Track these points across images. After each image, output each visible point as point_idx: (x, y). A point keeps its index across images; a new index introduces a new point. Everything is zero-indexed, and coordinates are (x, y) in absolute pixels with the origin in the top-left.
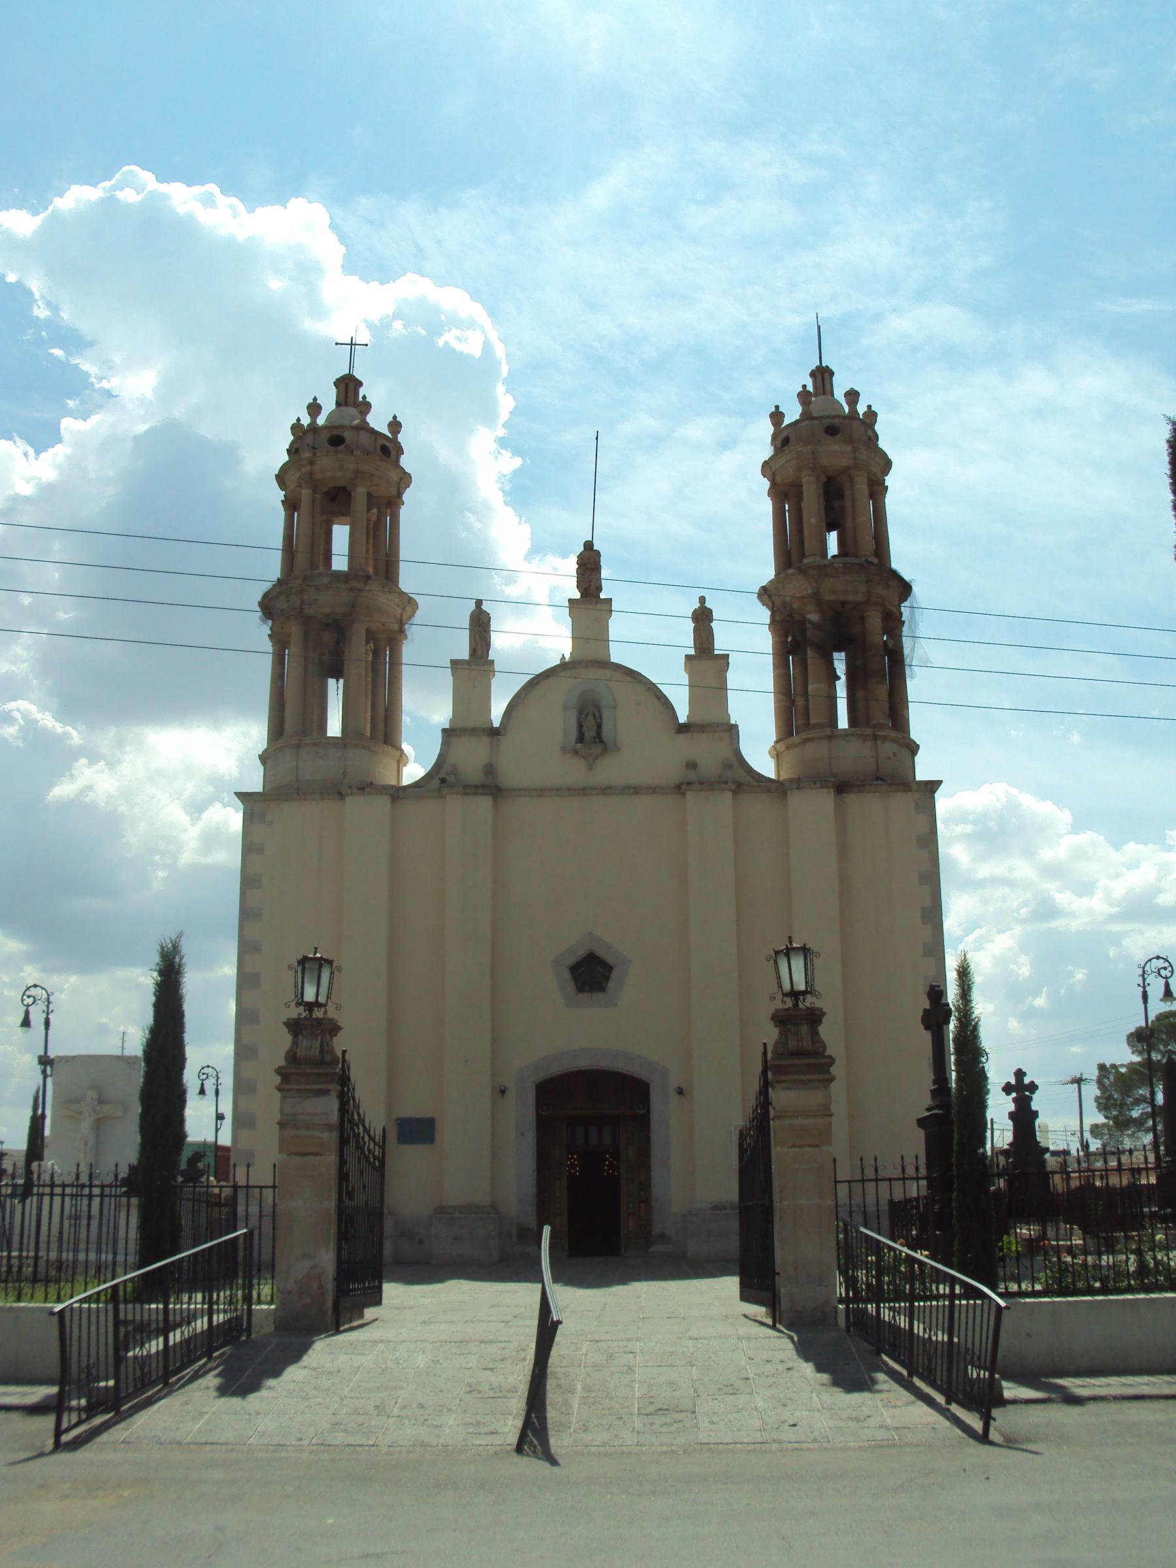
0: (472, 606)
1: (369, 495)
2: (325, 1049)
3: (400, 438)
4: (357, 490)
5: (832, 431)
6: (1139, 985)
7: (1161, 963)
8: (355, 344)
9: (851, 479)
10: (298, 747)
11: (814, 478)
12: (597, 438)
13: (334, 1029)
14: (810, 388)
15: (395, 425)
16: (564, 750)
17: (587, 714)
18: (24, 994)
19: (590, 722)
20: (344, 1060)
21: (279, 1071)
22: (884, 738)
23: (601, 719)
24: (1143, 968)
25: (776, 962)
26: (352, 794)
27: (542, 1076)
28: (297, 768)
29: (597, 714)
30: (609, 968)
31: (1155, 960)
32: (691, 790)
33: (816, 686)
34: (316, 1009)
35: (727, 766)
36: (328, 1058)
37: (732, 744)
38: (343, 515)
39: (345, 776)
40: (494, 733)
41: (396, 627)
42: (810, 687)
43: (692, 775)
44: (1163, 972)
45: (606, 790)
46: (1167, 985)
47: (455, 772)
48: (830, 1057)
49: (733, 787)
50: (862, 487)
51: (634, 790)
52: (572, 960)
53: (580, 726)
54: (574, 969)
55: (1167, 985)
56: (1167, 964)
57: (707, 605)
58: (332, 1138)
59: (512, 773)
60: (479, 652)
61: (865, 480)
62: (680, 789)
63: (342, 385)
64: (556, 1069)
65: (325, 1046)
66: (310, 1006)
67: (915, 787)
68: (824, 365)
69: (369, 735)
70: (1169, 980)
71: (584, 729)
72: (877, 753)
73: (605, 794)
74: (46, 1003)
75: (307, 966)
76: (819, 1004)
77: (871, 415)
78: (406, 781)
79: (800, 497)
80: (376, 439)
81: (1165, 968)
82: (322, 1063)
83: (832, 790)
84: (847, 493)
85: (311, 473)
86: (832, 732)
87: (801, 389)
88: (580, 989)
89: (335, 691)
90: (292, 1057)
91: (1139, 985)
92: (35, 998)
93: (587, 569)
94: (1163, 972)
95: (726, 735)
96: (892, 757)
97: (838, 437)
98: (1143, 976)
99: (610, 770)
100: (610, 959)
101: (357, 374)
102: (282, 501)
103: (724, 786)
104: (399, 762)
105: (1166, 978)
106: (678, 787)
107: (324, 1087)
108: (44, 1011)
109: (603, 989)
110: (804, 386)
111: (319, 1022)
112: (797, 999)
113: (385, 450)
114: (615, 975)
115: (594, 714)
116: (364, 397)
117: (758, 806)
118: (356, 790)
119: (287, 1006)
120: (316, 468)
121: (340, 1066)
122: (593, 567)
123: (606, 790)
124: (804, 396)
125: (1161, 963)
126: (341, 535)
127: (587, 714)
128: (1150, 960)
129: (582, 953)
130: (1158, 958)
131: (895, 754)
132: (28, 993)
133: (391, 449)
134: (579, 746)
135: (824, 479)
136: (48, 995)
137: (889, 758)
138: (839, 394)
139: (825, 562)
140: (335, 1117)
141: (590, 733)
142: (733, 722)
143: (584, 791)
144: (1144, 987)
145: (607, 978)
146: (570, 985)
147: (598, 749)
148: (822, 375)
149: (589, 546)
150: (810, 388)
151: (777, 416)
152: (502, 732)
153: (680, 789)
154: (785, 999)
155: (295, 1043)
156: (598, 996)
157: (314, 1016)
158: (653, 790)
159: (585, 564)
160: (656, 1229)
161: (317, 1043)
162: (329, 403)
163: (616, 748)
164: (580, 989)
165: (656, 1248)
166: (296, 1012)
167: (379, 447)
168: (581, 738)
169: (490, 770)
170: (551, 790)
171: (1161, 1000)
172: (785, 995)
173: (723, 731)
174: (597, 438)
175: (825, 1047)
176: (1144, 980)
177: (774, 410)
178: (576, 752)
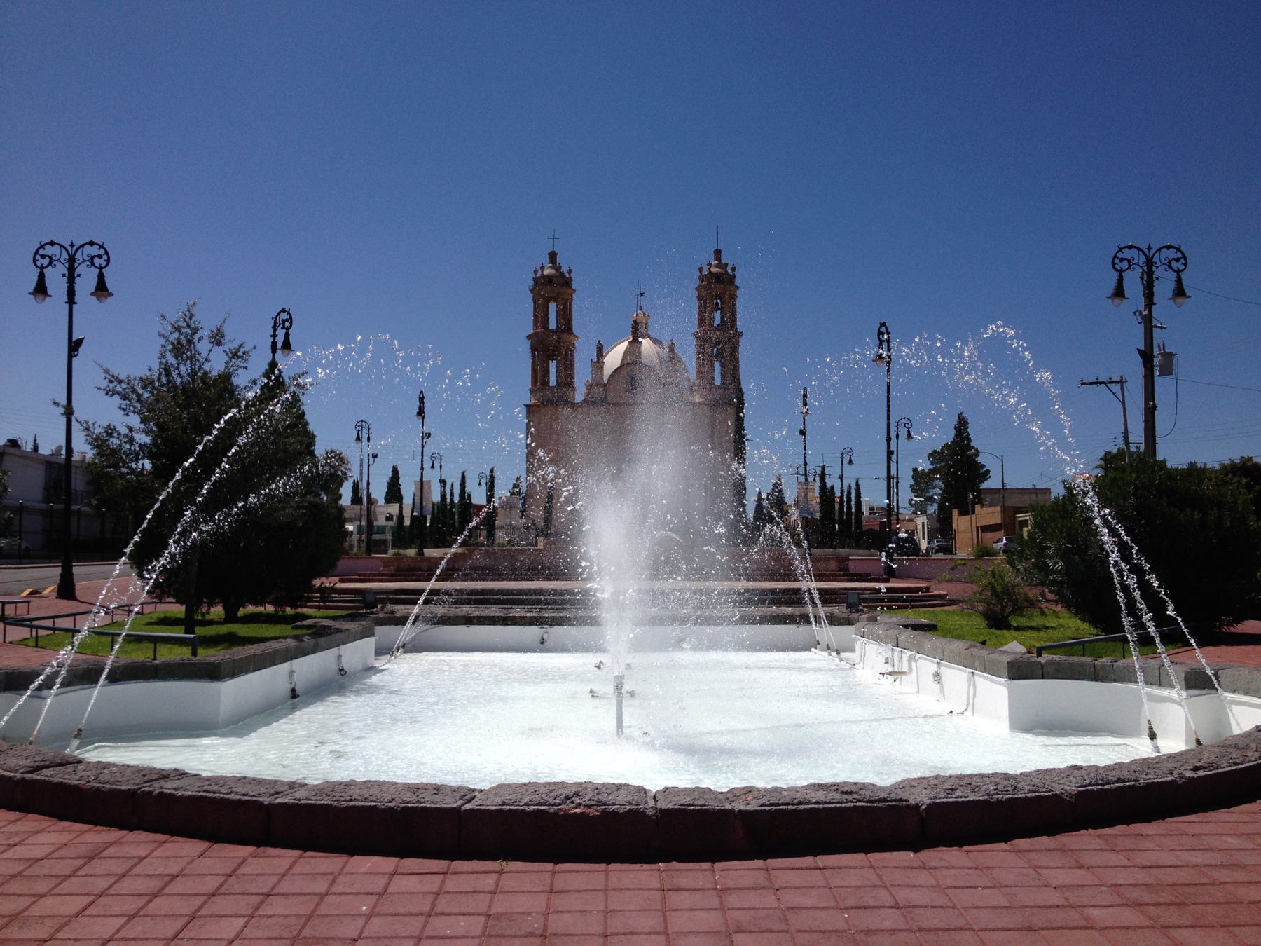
15: (570, 271)
40: (604, 385)
77: (733, 269)
89: (553, 365)
126: (553, 307)
151: (701, 269)
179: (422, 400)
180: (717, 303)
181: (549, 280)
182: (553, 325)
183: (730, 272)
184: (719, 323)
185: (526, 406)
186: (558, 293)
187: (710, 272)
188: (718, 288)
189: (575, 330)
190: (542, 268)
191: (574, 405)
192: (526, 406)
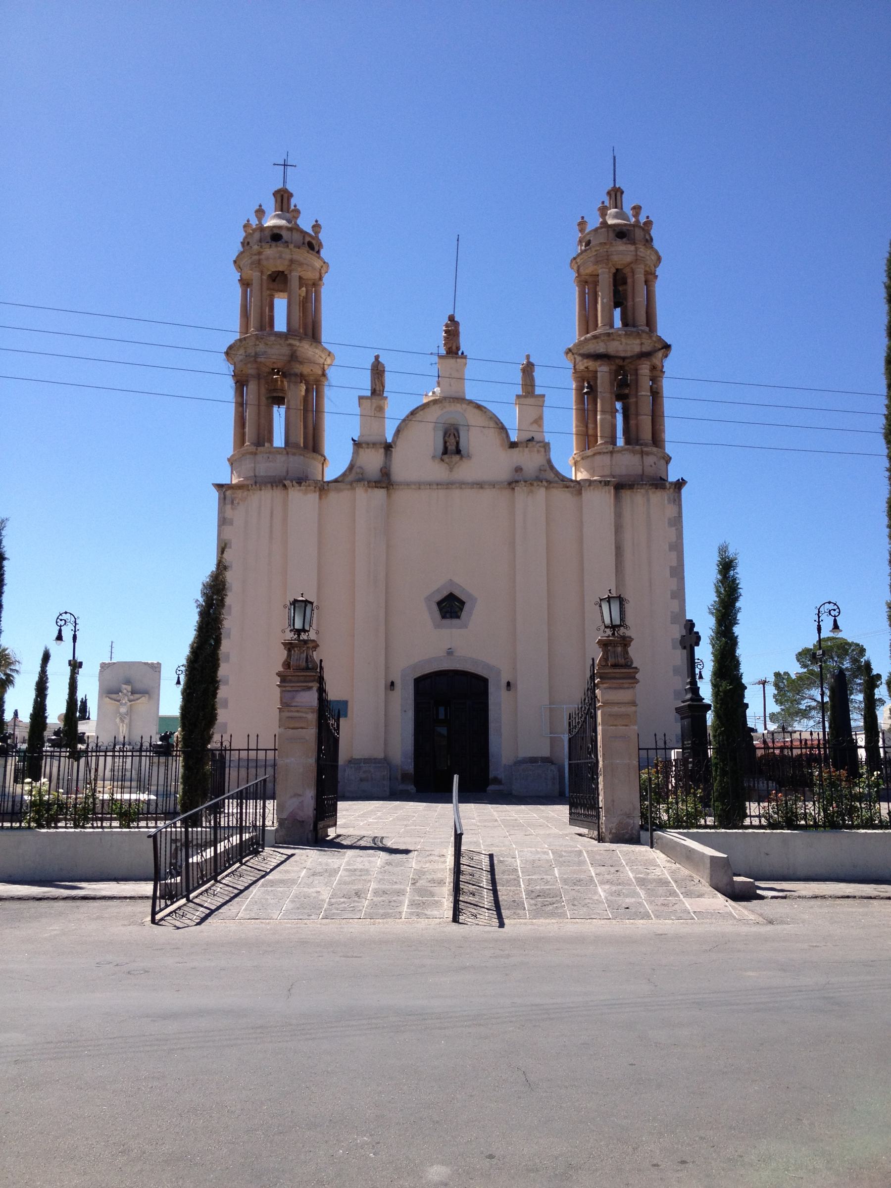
0: (373, 360)
1: (300, 278)
3: (321, 236)
4: (292, 274)
7: (831, 606)
8: (287, 165)
9: (633, 272)
10: (255, 454)
11: (607, 270)
15: (317, 227)
16: (434, 457)
17: (450, 434)
18: (58, 618)
19: (452, 441)
20: (321, 668)
21: (279, 674)
22: (648, 454)
23: (459, 438)
24: (819, 609)
25: (601, 606)
28: (255, 467)
29: (456, 435)
30: (463, 603)
32: (518, 486)
34: (302, 633)
35: (541, 470)
36: (310, 666)
38: (281, 291)
40: (388, 448)
41: (320, 372)
44: (833, 613)
45: (462, 485)
46: (835, 621)
48: (636, 668)
50: (640, 277)
51: (480, 485)
52: (439, 597)
53: (445, 443)
54: (439, 604)
55: (835, 621)
56: (835, 607)
57: (531, 360)
58: (312, 717)
62: (512, 484)
65: (309, 657)
66: (298, 632)
68: (617, 186)
69: (302, 445)
71: (448, 444)
72: (643, 462)
73: (461, 488)
74: (74, 624)
75: (296, 605)
76: (628, 633)
77: (649, 223)
78: (327, 478)
79: (596, 283)
80: (304, 237)
81: (834, 610)
82: (307, 669)
83: (612, 488)
84: (629, 281)
86: (613, 448)
88: (444, 617)
89: (279, 415)
90: (287, 664)
92: (65, 621)
94: (833, 613)
96: (653, 465)
97: (624, 240)
98: (818, 615)
100: (463, 598)
101: (290, 188)
104: (323, 464)
106: (510, 484)
108: (72, 630)
109: (458, 617)
110: (603, 203)
111: (305, 642)
112: (614, 630)
113: (311, 246)
114: (466, 608)
115: (454, 434)
116: (295, 206)
117: (561, 496)
120: (263, 257)
121: (318, 670)
123: (462, 485)
125: (831, 606)
126: (281, 305)
127: (450, 434)
128: (824, 604)
129: (445, 593)
130: (830, 603)
131: (655, 463)
132: (60, 617)
133: (315, 244)
135: (613, 270)
136: (75, 619)
137: (651, 466)
138: (627, 209)
140: (315, 703)
141: (452, 447)
142: (547, 441)
143: (448, 485)
144: (819, 622)
145: (461, 610)
147: (456, 458)
149: (452, 318)
150: (607, 204)
151: (582, 224)
152: (393, 446)
153: (512, 484)
154: (606, 629)
155: (289, 655)
157: (301, 638)
158: (493, 485)
160: (491, 776)
163: (469, 457)
164: (444, 617)
165: (491, 788)
166: (290, 636)
168: (445, 452)
171: (830, 631)
172: (606, 627)
175: (632, 663)
176: (819, 617)
178: (442, 460)
181: (275, 236)
182: (280, 325)
185: (219, 487)
186: (292, 261)
187: (604, 224)
188: (623, 252)
189: (327, 334)
190: (260, 212)
191: (323, 488)
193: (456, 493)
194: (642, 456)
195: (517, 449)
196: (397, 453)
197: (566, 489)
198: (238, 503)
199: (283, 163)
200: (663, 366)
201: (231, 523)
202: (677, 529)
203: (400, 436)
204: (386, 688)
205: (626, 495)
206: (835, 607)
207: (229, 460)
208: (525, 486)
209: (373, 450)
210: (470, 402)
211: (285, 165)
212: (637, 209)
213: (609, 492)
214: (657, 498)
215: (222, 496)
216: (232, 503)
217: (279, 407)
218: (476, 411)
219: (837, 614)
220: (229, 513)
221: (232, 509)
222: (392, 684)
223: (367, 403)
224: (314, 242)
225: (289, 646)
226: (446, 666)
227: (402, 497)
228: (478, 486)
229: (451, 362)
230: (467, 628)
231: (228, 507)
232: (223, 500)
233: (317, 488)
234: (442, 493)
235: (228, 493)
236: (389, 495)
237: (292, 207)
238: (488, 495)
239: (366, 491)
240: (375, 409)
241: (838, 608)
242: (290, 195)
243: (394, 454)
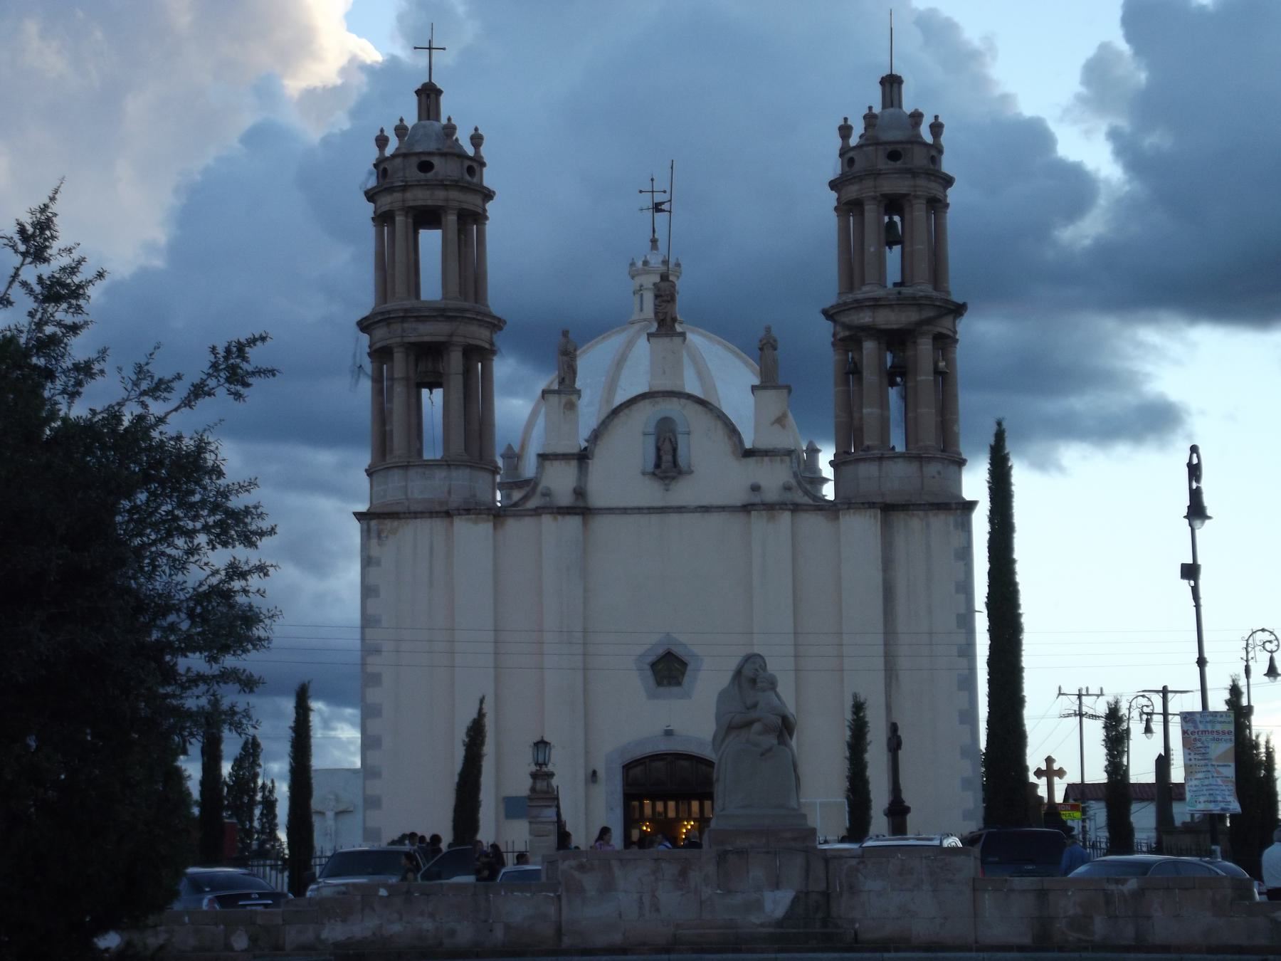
2: (549, 785)
3: (484, 151)
4: (449, 218)
5: (894, 156)
6: (1242, 658)
7: (1266, 636)
12: (672, 168)
13: (551, 775)
14: (877, 109)
15: (477, 140)
17: (665, 439)
19: (667, 447)
23: (677, 444)
24: (1247, 640)
26: (459, 514)
27: (628, 757)
29: (673, 440)
30: (684, 665)
31: (1261, 632)
32: (755, 510)
33: (869, 410)
34: (544, 766)
35: (787, 488)
37: (792, 467)
39: (449, 493)
40: (583, 457)
42: (864, 411)
43: (756, 499)
44: (1268, 646)
45: (680, 510)
46: (1272, 659)
47: (547, 494)
49: (791, 507)
51: (706, 509)
52: (651, 659)
53: (658, 449)
54: (654, 665)
55: (1272, 659)
56: (1272, 638)
59: (599, 495)
60: (567, 382)
61: (924, 207)
62: (747, 508)
63: (424, 96)
64: (639, 753)
67: (954, 506)
68: (893, 73)
70: (1274, 654)
71: (662, 452)
73: (681, 512)
77: (936, 128)
79: (862, 213)
81: (1270, 642)
83: (879, 512)
85: (404, 201)
87: (868, 112)
88: (659, 683)
89: (432, 401)
91: (1242, 658)
93: (663, 301)
94: (1268, 646)
95: (787, 459)
98: (1246, 649)
99: (684, 492)
100: (685, 659)
102: (372, 218)
103: (784, 507)
105: (1271, 652)
107: (550, 804)
109: (679, 684)
110: (870, 108)
115: (670, 440)
116: (449, 119)
117: (813, 524)
118: (461, 512)
119: (529, 765)
122: (669, 298)
123: (680, 510)
124: (870, 118)
125: (1266, 636)
127: (665, 439)
129: (661, 651)
130: (1263, 630)
134: (657, 472)
137: (934, 477)
138: (908, 107)
139: (880, 293)
144: (1247, 661)
145: (683, 674)
146: (651, 681)
148: (891, 84)
150: (877, 109)
151: (845, 131)
152: (590, 457)
153: (747, 508)
155: (534, 783)
156: (675, 690)
157: (543, 770)
158: (722, 509)
159: (661, 296)
161: (545, 784)
162: (411, 120)
163: (690, 472)
164: (659, 683)
166: (534, 768)
167: (465, 170)
168: (658, 466)
169: (580, 493)
170: (631, 509)
171: (1265, 675)
173: (785, 455)
174: (672, 168)
176: (1247, 653)
177: (843, 123)
178: (654, 474)
179: (1194, 471)
180: (892, 224)
183: (927, 137)
184: (898, 279)
185: (359, 516)
192: (359, 516)
193: (674, 518)
194: (921, 467)
195: (754, 458)
196: (596, 467)
197: (819, 512)
198: (387, 537)
199: (428, 50)
200: (955, 332)
201: (378, 563)
202: (965, 565)
203: (598, 442)
204: (587, 782)
205: (899, 519)
206: (1272, 638)
207: (366, 470)
208: (764, 510)
209: (563, 462)
210: (690, 397)
211: (430, 48)
212: (917, 117)
213: (875, 517)
214: (939, 522)
215: (365, 527)
216: (379, 537)
217: (431, 393)
218: (698, 407)
219: (1275, 648)
220: (375, 551)
221: (379, 545)
222: (594, 773)
223: (554, 399)
224: (475, 165)
225: (534, 776)
226: (664, 746)
227: (601, 525)
228: (703, 509)
229: (664, 343)
230: (691, 698)
231: (374, 542)
232: (366, 535)
233: (491, 517)
234: (655, 518)
235: (373, 523)
236: (585, 524)
237: (444, 121)
238: (715, 520)
239: (555, 519)
240: (564, 407)
241: (1277, 639)
242: (439, 92)
243: (590, 466)
